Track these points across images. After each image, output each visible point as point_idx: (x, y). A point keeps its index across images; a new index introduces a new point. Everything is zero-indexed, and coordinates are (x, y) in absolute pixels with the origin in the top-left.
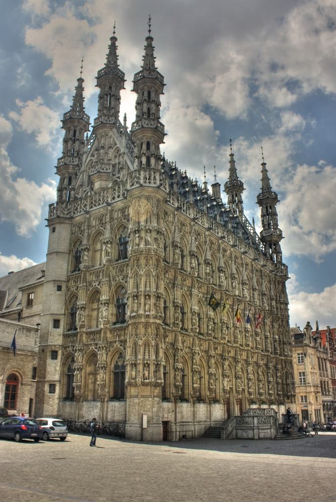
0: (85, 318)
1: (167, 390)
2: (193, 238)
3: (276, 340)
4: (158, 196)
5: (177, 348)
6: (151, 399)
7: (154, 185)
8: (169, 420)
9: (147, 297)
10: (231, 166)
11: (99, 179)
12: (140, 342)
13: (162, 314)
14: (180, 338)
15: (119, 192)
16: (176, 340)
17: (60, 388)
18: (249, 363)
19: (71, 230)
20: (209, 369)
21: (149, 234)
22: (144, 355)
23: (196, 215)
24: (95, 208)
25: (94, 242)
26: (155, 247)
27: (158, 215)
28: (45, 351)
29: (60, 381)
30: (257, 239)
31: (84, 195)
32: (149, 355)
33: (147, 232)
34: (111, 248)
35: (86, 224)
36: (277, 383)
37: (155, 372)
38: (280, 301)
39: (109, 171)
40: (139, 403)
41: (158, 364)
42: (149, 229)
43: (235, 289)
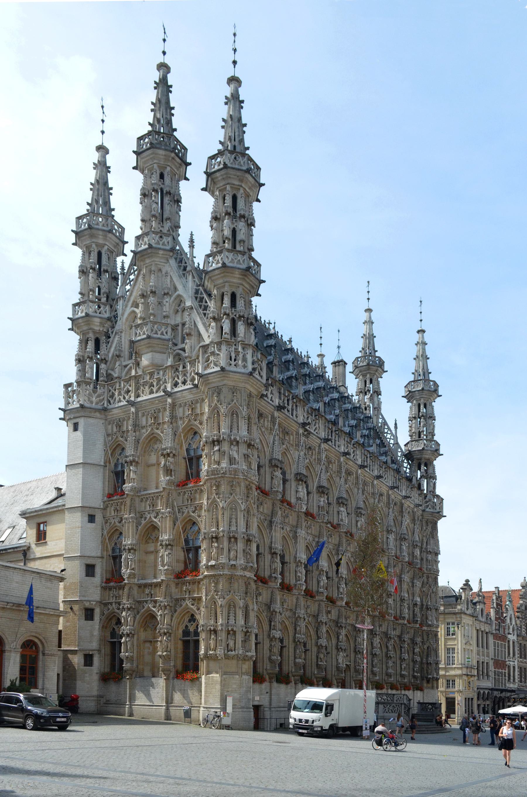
2: (302, 453)
4: (249, 387)
7: (243, 370)
9: (233, 540)
13: (253, 564)
14: (278, 598)
15: (185, 375)
16: (272, 600)
21: (236, 448)
22: (228, 619)
23: (308, 418)
26: (244, 467)
29: (99, 651)
31: (124, 374)
32: (235, 620)
33: (232, 444)
35: (131, 422)
37: (244, 641)
41: (247, 632)
42: (235, 439)
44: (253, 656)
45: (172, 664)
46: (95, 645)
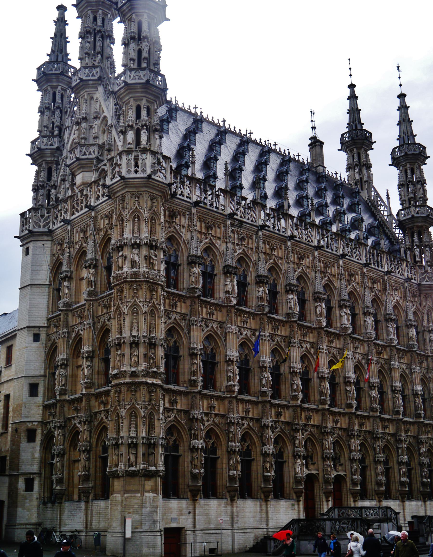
0: (66, 380)
1: (181, 481)
3: (417, 394)
5: (194, 417)
6: (139, 495)
8: (181, 526)
10: (350, 104)
11: (81, 170)
12: (123, 412)
13: (158, 368)
17: (40, 484)
18: (352, 434)
19: (52, 250)
20: (263, 446)
21: (136, 251)
24: (77, 214)
25: (77, 266)
26: (146, 269)
27: (152, 219)
28: (19, 431)
29: (39, 474)
30: (394, 225)
32: (137, 431)
34: (95, 274)
36: (422, 465)
38: (428, 327)
39: (94, 156)
40: (122, 502)
43: (321, 316)
44: (157, 472)
45: (90, 485)
46: (35, 468)
